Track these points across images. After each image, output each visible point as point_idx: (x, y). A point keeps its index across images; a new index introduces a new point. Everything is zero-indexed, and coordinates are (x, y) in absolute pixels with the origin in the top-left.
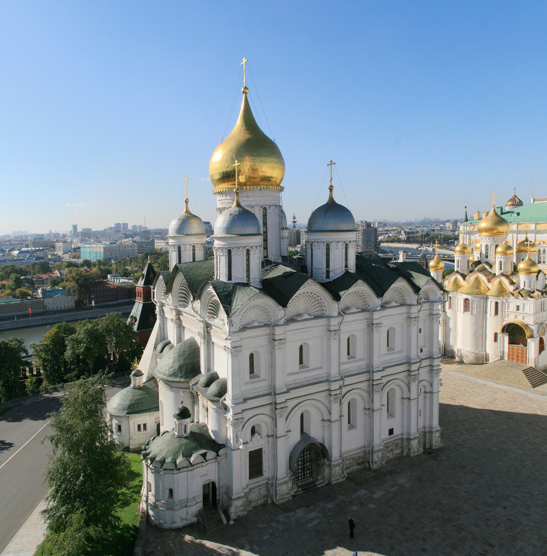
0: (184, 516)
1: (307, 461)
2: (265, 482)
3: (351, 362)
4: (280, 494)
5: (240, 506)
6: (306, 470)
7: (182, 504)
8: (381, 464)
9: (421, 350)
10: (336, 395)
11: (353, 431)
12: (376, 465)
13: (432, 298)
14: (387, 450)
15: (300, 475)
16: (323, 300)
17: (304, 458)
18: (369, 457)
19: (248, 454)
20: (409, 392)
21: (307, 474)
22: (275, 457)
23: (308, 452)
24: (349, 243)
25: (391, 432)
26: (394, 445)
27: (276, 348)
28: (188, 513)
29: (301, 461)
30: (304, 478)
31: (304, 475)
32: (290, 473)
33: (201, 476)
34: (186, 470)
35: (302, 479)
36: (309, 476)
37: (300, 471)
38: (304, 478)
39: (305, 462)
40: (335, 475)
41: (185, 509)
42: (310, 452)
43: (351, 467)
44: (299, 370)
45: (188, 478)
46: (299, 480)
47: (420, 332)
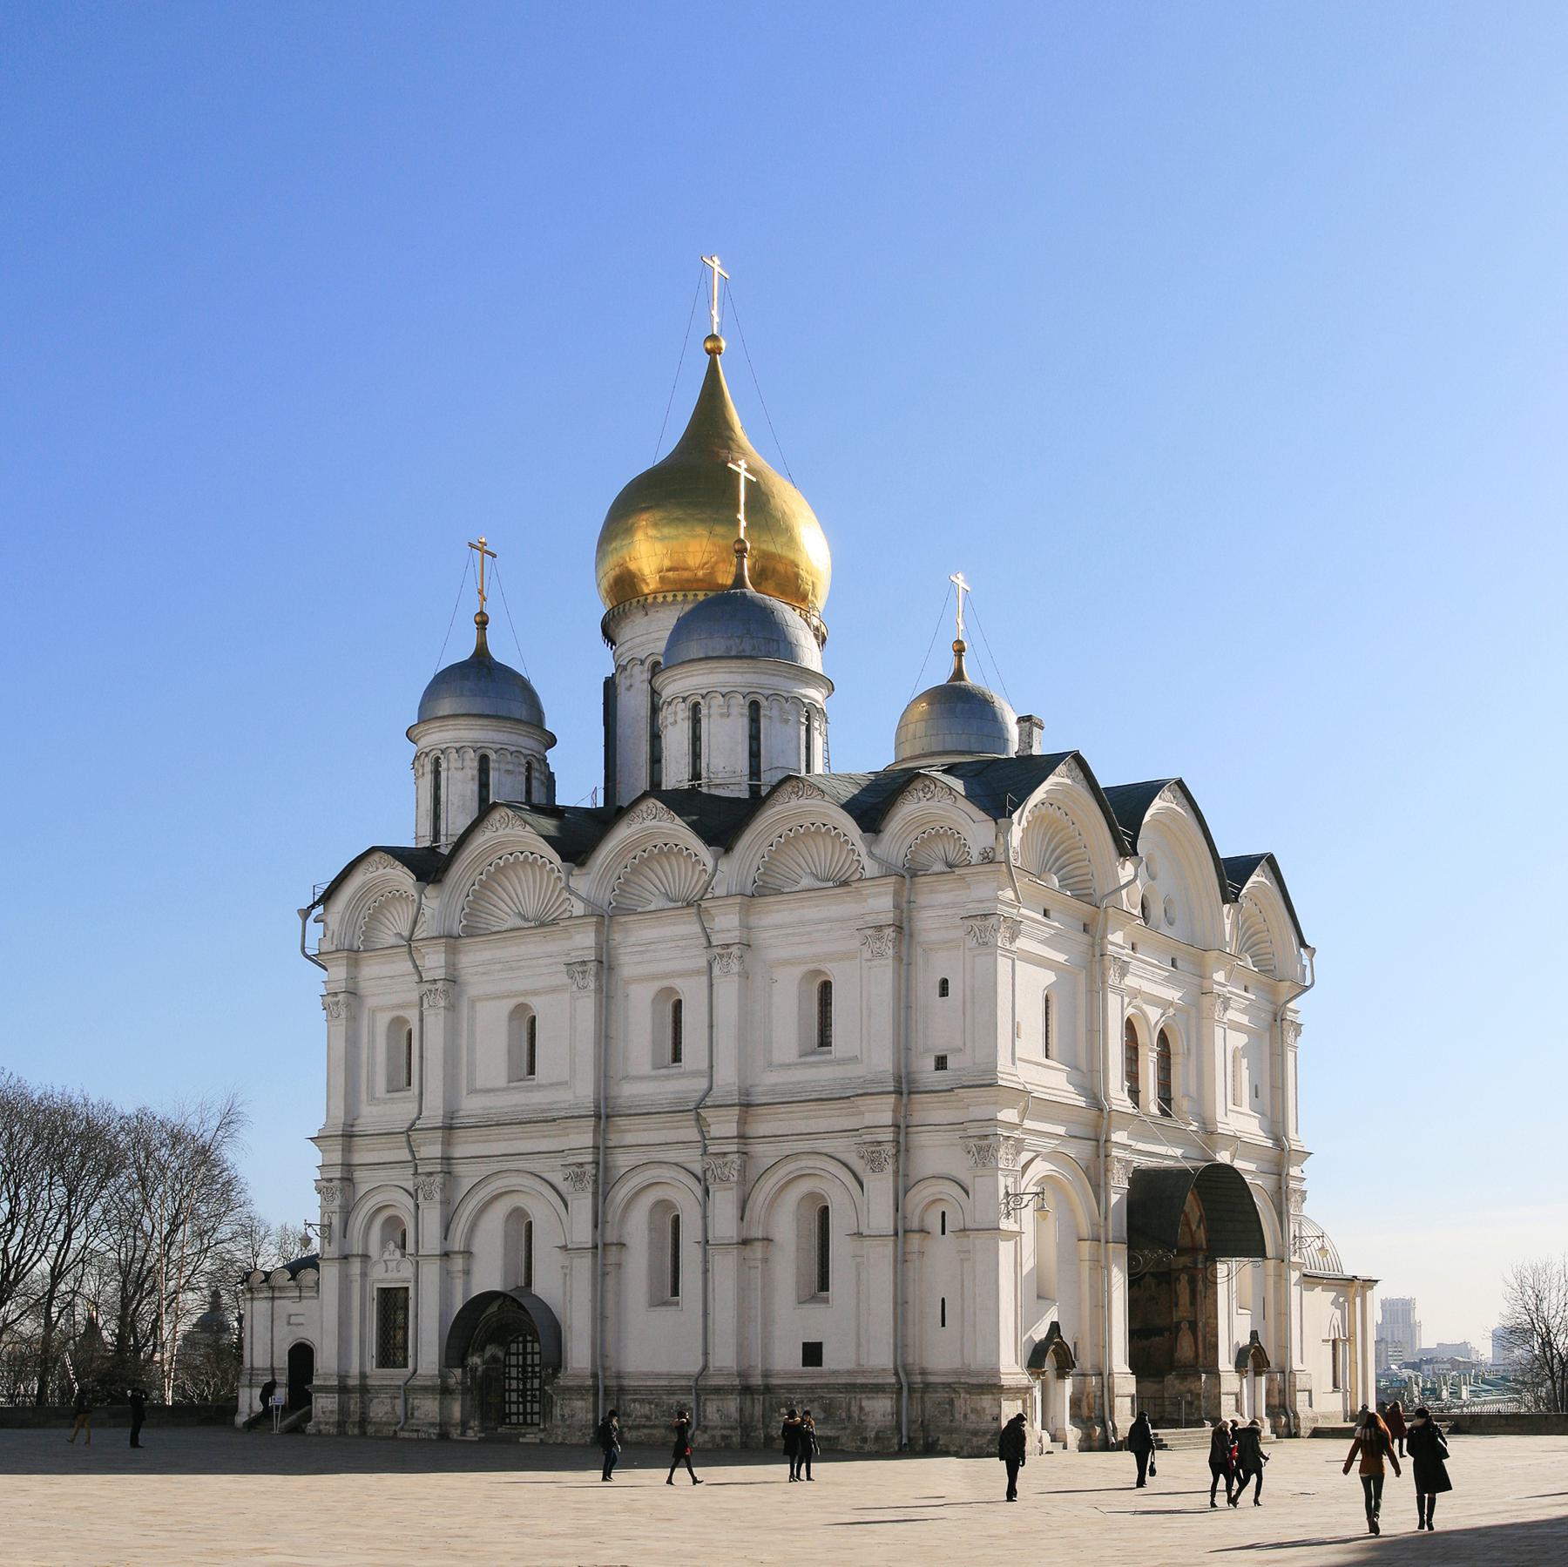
1: (533, 1372)
3: (655, 1078)
6: (529, 1398)
8: (724, 1437)
9: (941, 1063)
10: (581, 1164)
11: (665, 1315)
12: (706, 1437)
17: (525, 1359)
21: (532, 1413)
25: (812, 1354)
29: (518, 1366)
31: (525, 1414)
35: (518, 1424)
37: (514, 1396)
39: (527, 1372)
43: (645, 1426)
44: (505, 1085)
46: (510, 1423)
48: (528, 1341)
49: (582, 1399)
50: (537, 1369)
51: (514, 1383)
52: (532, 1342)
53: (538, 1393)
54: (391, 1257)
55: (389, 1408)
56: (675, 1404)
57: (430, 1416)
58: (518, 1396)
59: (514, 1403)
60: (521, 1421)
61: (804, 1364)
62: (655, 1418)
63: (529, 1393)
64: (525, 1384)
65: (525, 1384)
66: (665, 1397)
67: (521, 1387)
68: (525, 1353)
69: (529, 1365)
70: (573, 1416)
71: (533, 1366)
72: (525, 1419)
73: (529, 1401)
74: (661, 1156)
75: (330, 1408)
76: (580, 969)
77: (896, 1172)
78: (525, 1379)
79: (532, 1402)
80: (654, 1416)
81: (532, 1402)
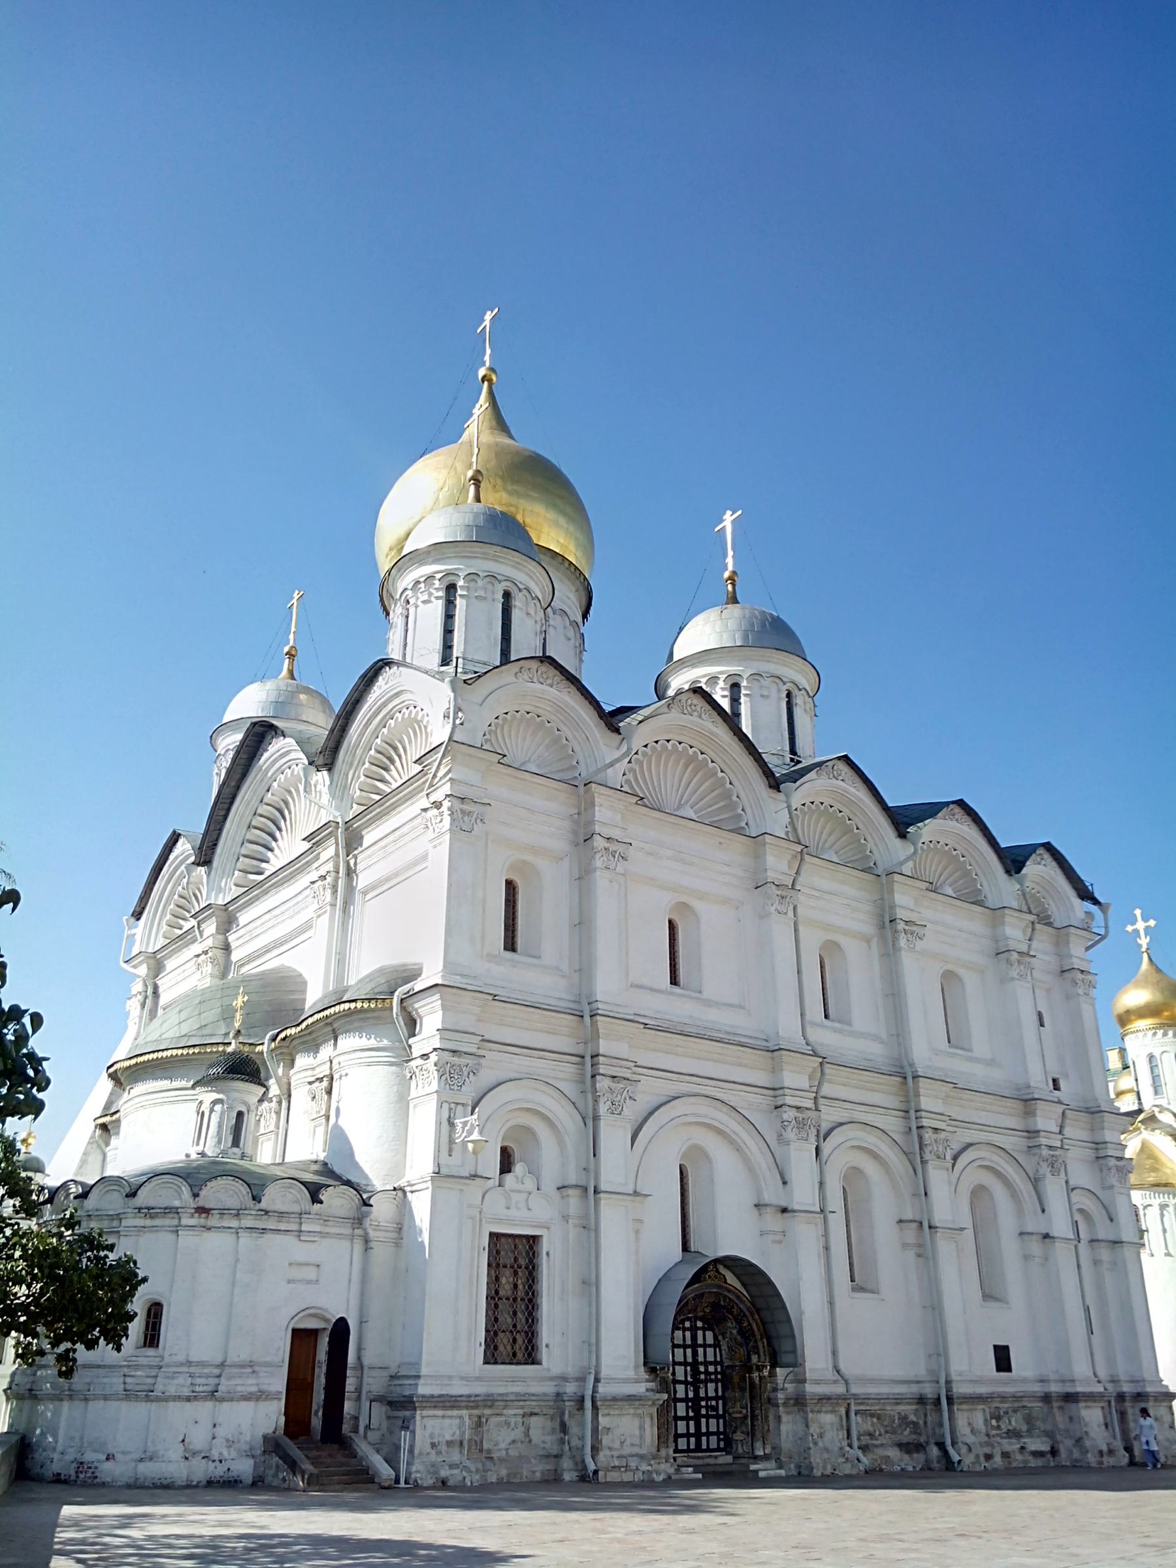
0: (199, 1439)
1: (706, 1370)
2: (549, 1388)
4: (610, 1449)
5: (449, 1443)
6: (703, 1411)
7: (198, 1381)
13: (1059, 920)
14: (999, 1427)
15: (682, 1427)
16: (739, 787)
17: (695, 1354)
18: (941, 1425)
19: (485, 1241)
20: (1043, 1211)
22: (590, 1285)
23: (710, 1335)
24: (795, 692)
26: (1019, 1415)
27: (599, 862)
28: (218, 1430)
30: (698, 1448)
31: (698, 1435)
32: (647, 1381)
33: (289, 1282)
34: (234, 1223)
35: (688, 1450)
36: (718, 1449)
37: (681, 1410)
38: (698, 1448)
40: (821, 1444)
41: (209, 1405)
42: (715, 1338)
45: (237, 1260)
47: (1042, 1025)
48: (698, 1329)
49: (832, 1412)
50: (711, 1369)
51: (680, 1389)
52: (704, 1329)
53: (714, 1403)
54: (520, 1187)
55: (518, 1433)
56: (897, 1418)
57: (628, 1442)
58: (687, 1408)
59: (682, 1418)
60: (692, 1446)
61: (999, 1369)
62: (880, 1435)
63: (703, 1403)
64: (696, 1392)
65: (696, 1392)
66: (888, 1408)
67: (691, 1395)
68: (694, 1346)
69: (701, 1363)
70: (821, 1436)
71: (706, 1363)
72: (698, 1443)
73: (704, 1416)
74: (863, 1117)
75: (448, 1437)
76: (779, 892)
77: (1067, 1182)
78: (696, 1383)
79: (707, 1417)
80: (877, 1433)
81: (707, 1417)
